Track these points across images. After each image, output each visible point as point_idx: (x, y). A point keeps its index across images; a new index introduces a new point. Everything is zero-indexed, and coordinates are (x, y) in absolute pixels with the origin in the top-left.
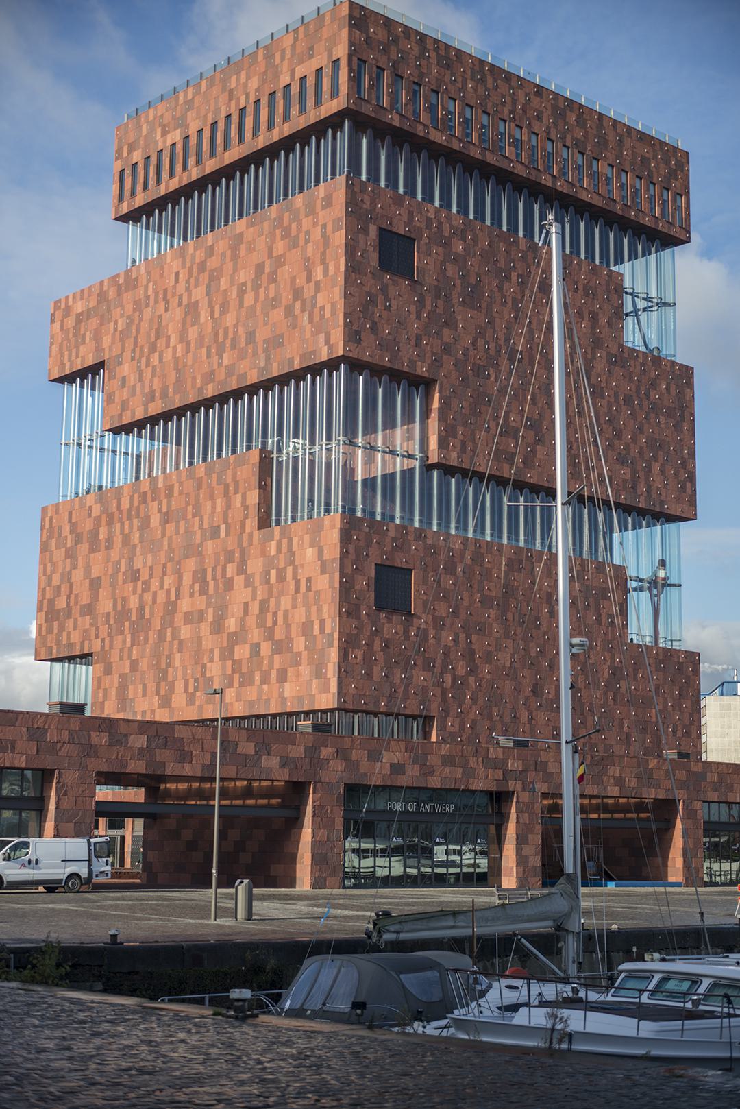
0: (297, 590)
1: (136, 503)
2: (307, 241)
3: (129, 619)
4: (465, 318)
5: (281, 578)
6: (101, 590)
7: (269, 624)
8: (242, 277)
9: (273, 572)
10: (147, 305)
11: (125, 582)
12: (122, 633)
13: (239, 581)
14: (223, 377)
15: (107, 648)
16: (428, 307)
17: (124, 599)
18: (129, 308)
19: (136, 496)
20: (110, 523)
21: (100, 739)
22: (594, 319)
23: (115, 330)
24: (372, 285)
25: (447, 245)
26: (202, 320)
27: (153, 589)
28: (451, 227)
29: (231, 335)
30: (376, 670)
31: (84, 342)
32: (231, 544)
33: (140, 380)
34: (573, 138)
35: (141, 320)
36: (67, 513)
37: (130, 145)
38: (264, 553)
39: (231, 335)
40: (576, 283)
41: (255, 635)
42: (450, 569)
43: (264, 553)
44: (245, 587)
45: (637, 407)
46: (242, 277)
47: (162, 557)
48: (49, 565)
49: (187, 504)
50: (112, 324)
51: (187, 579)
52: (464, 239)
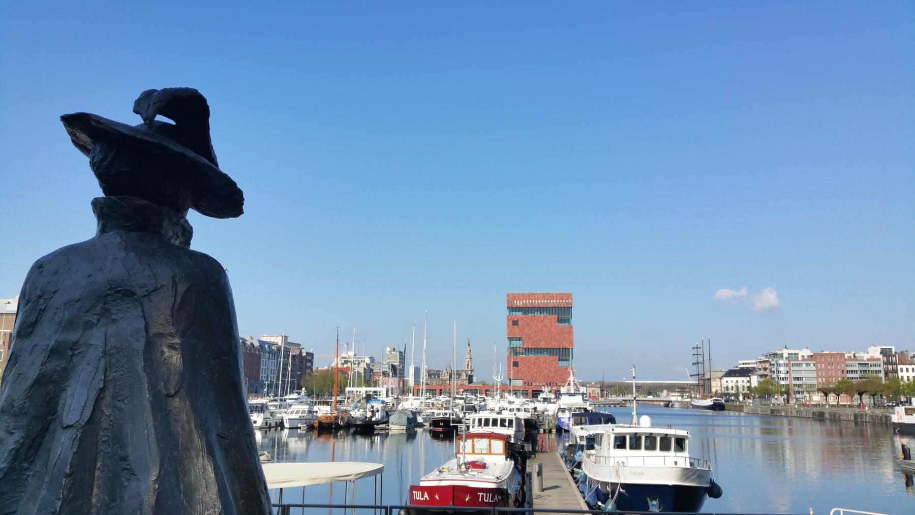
22: (551, 323)
24: (511, 328)
42: (525, 360)
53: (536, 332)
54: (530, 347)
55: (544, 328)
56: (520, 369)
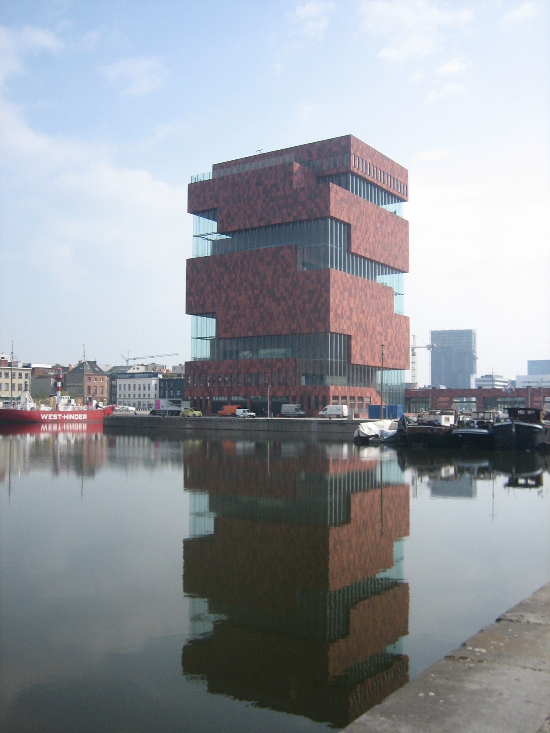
3: (362, 327)
12: (360, 331)
13: (390, 326)
15: (356, 335)
17: (360, 319)
41: (394, 344)
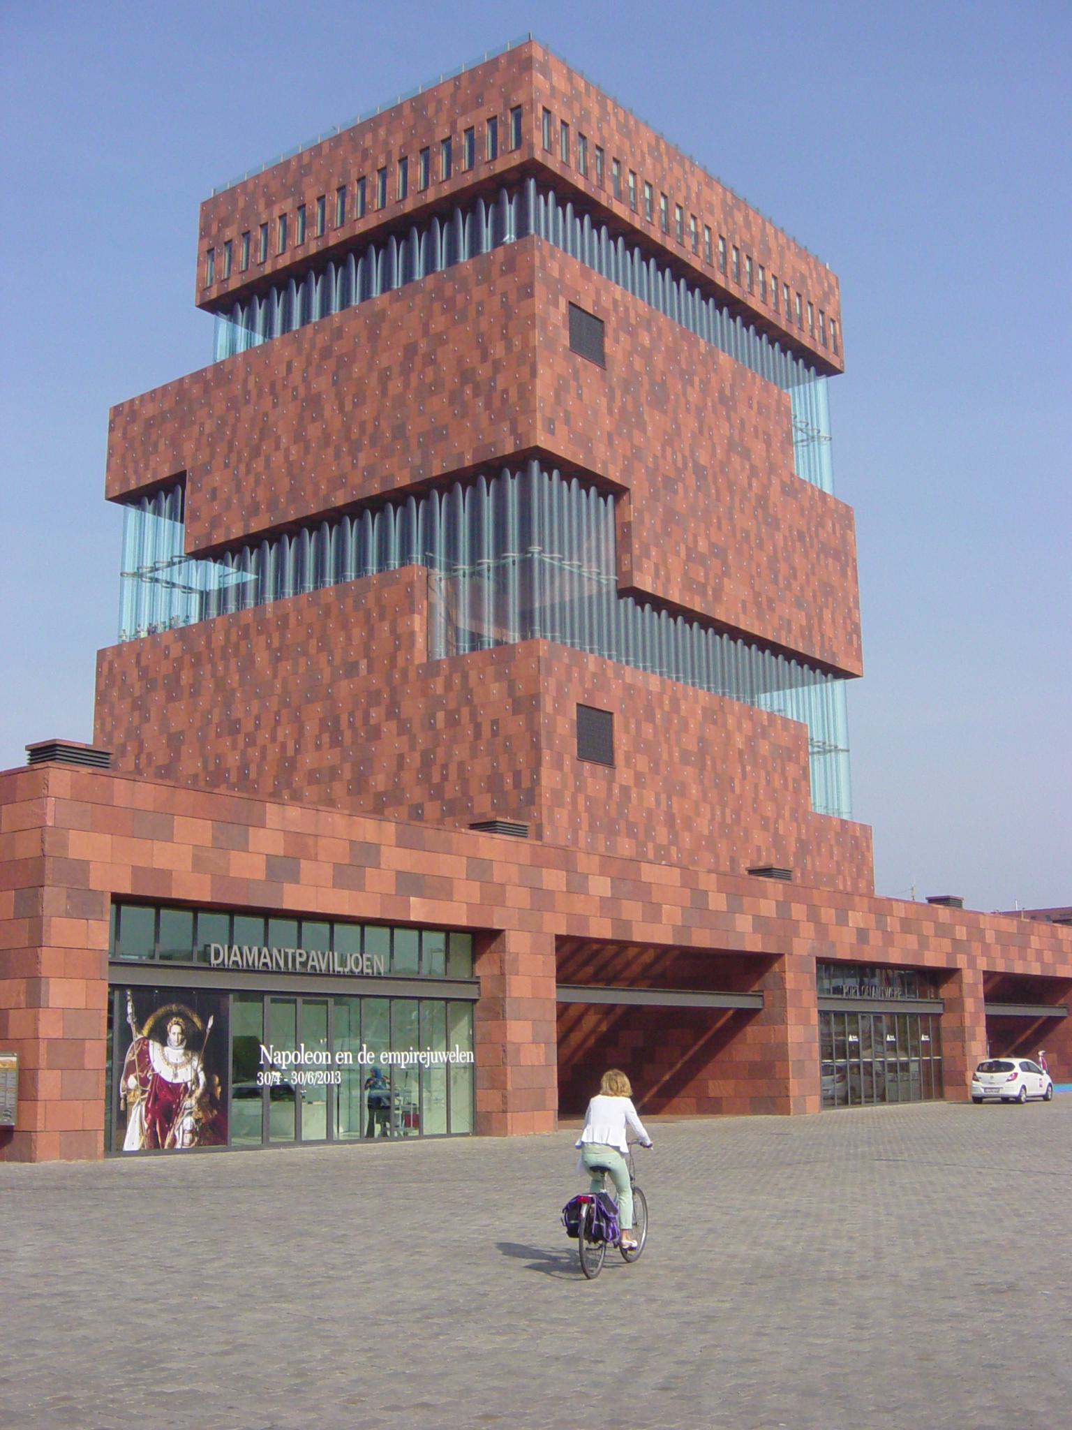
0: (478, 735)
1: (234, 638)
2: (479, 313)
4: (654, 420)
5: (452, 722)
6: (184, 748)
7: (436, 779)
8: (384, 360)
9: (440, 716)
10: (247, 402)
11: (218, 736)
13: (389, 728)
14: (357, 479)
16: (618, 402)
17: (218, 756)
18: (220, 407)
19: (234, 631)
20: (197, 665)
21: (554, 879)
22: (768, 443)
23: (201, 433)
25: (633, 334)
26: (327, 414)
27: (260, 742)
28: (637, 315)
29: (370, 429)
30: (582, 834)
31: (156, 451)
32: (376, 681)
33: (239, 489)
34: (742, 240)
35: (238, 420)
36: (134, 656)
37: (220, 221)
38: (425, 692)
39: (370, 429)
40: (750, 398)
41: (415, 794)
42: (650, 717)
43: (425, 692)
44: (399, 735)
45: (808, 545)
46: (384, 360)
47: (273, 704)
48: (109, 720)
49: (310, 636)
50: (196, 428)
51: (311, 728)
52: (649, 330)
53: (699, 471)
54: (675, 596)
55: (735, 459)
56: (625, 790)
